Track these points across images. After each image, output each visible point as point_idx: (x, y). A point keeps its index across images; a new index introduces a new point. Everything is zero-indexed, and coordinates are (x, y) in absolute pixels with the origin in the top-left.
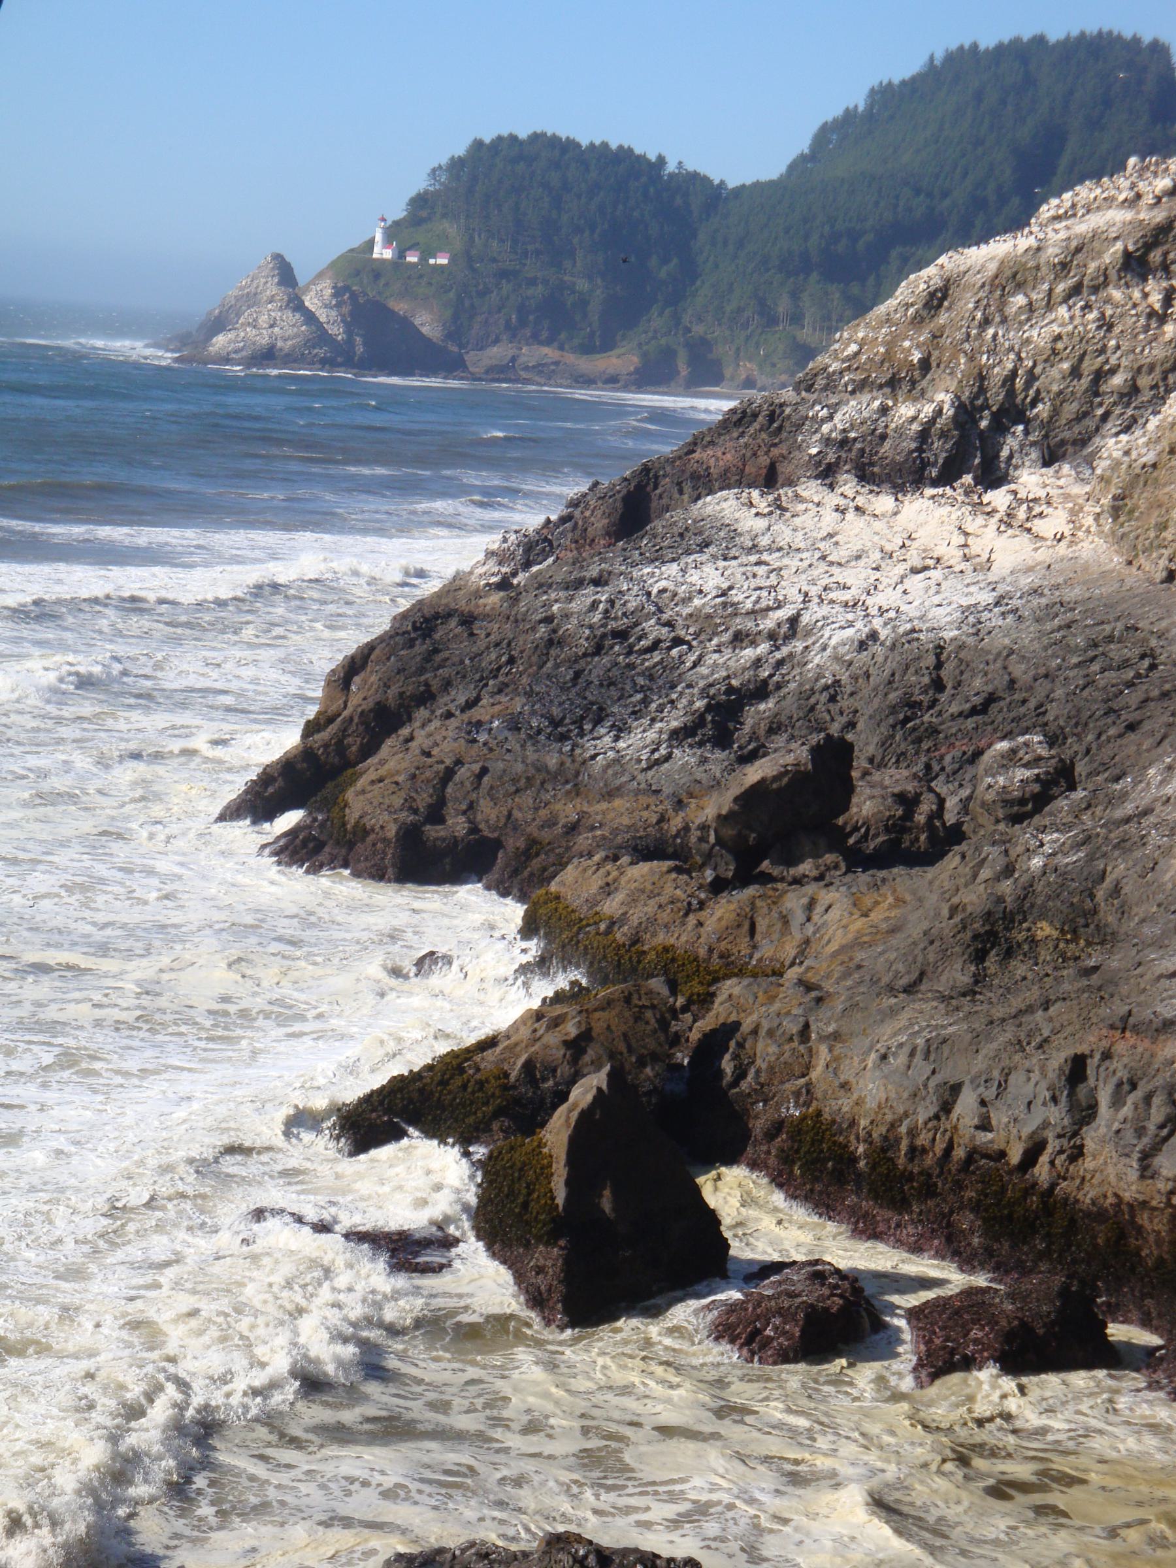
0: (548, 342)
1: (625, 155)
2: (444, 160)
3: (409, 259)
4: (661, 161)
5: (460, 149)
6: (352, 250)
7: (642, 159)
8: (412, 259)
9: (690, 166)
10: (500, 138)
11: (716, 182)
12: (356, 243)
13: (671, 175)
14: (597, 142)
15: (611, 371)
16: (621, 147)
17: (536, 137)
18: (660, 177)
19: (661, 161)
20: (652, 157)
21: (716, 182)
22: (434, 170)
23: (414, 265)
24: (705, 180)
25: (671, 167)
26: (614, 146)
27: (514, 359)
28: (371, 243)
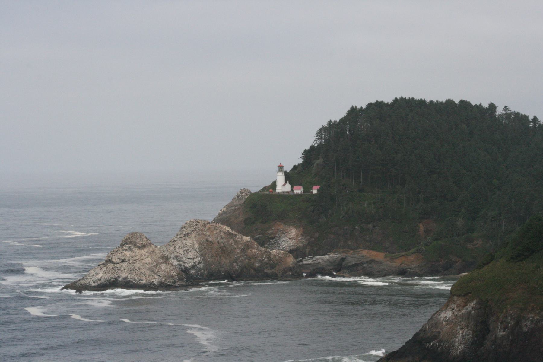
0: (374, 246)
1: (464, 104)
2: (325, 124)
3: (295, 191)
4: (492, 107)
5: (338, 114)
6: (264, 188)
7: (479, 108)
8: (298, 191)
9: (513, 108)
10: (370, 105)
11: (531, 118)
12: (269, 183)
13: (499, 115)
14: (435, 101)
15: (404, 266)
16: (462, 102)
17: (396, 100)
18: (495, 116)
19: (492, 107)
20: (486, 105)
21: (531, 118)
22: (320, 129)
23: (297, 195)
24: (526, 117)
25: (500, 111)
26: (457, 102)
27: (343, 259)
28: (274, 185)
